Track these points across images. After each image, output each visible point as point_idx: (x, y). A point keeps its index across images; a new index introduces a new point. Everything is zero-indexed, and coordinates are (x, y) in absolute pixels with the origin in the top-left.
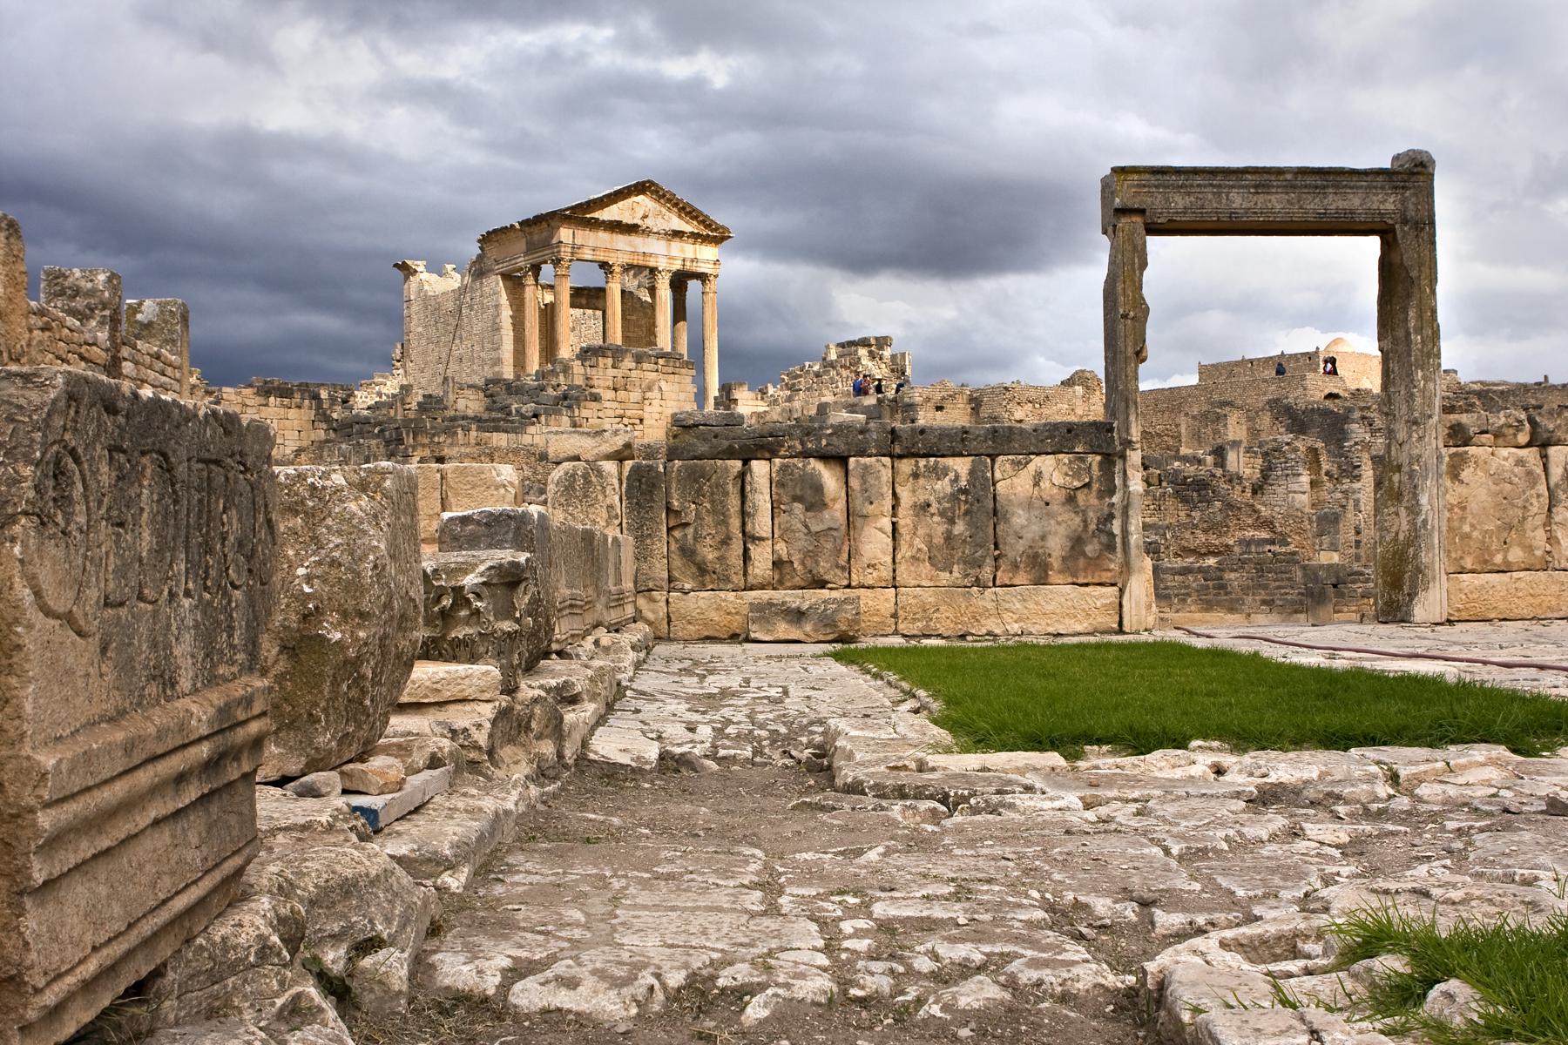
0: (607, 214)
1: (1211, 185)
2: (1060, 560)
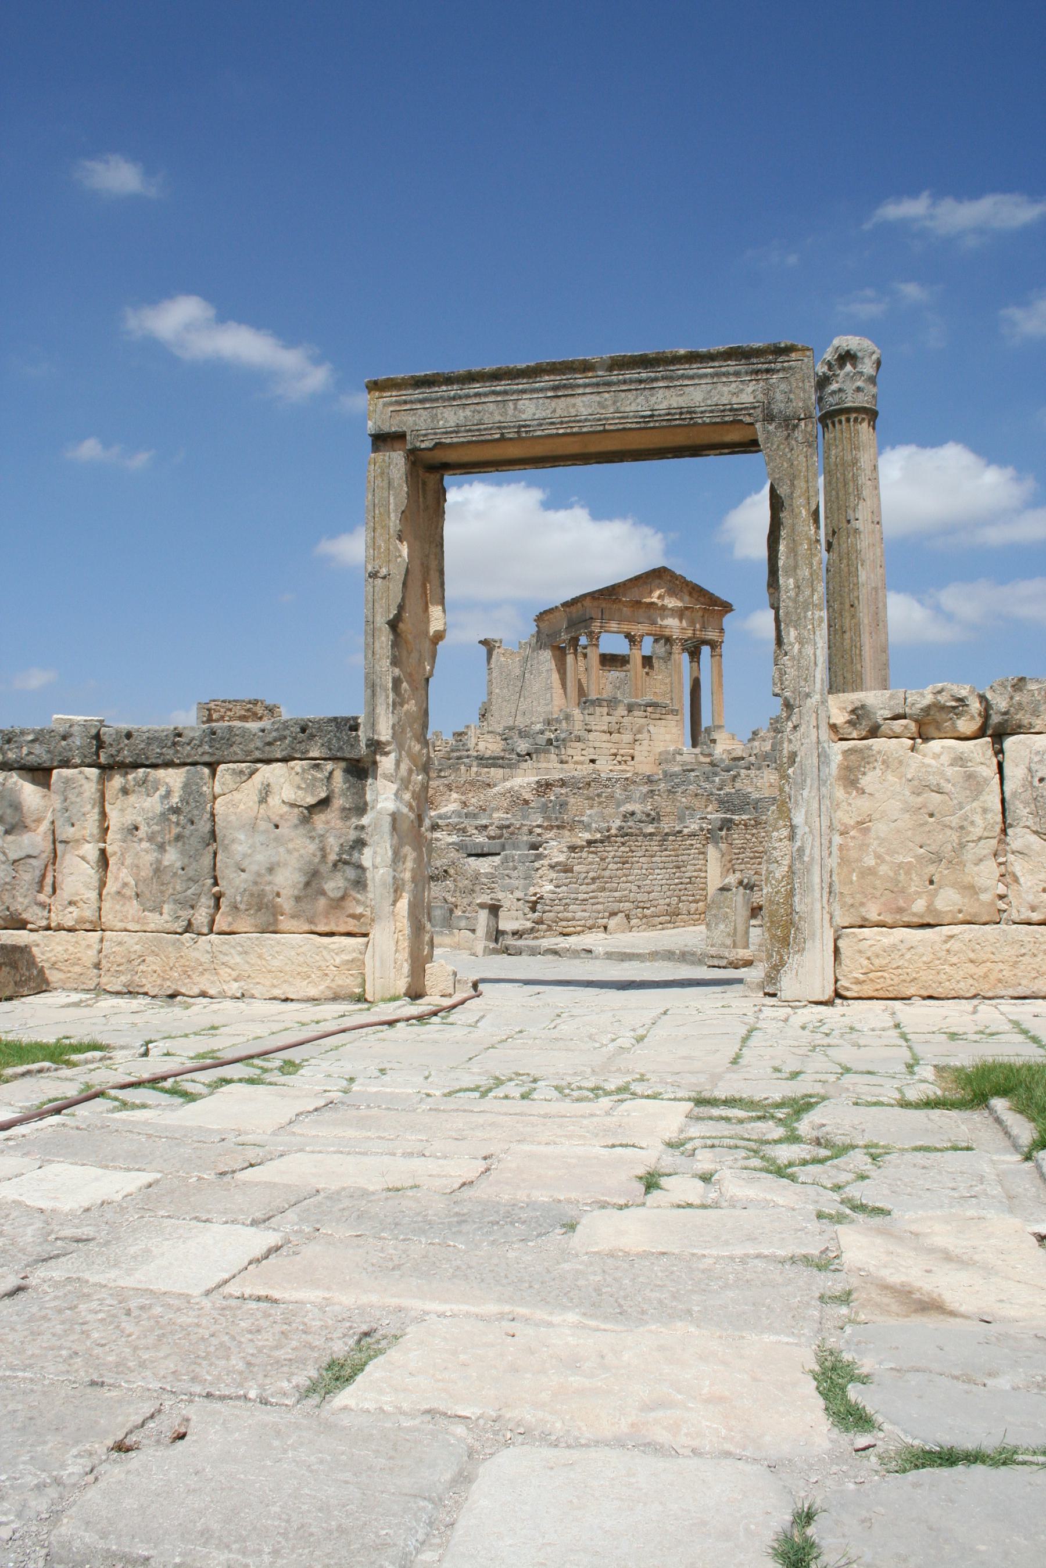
1: (494, 393)
2: (292, 902)
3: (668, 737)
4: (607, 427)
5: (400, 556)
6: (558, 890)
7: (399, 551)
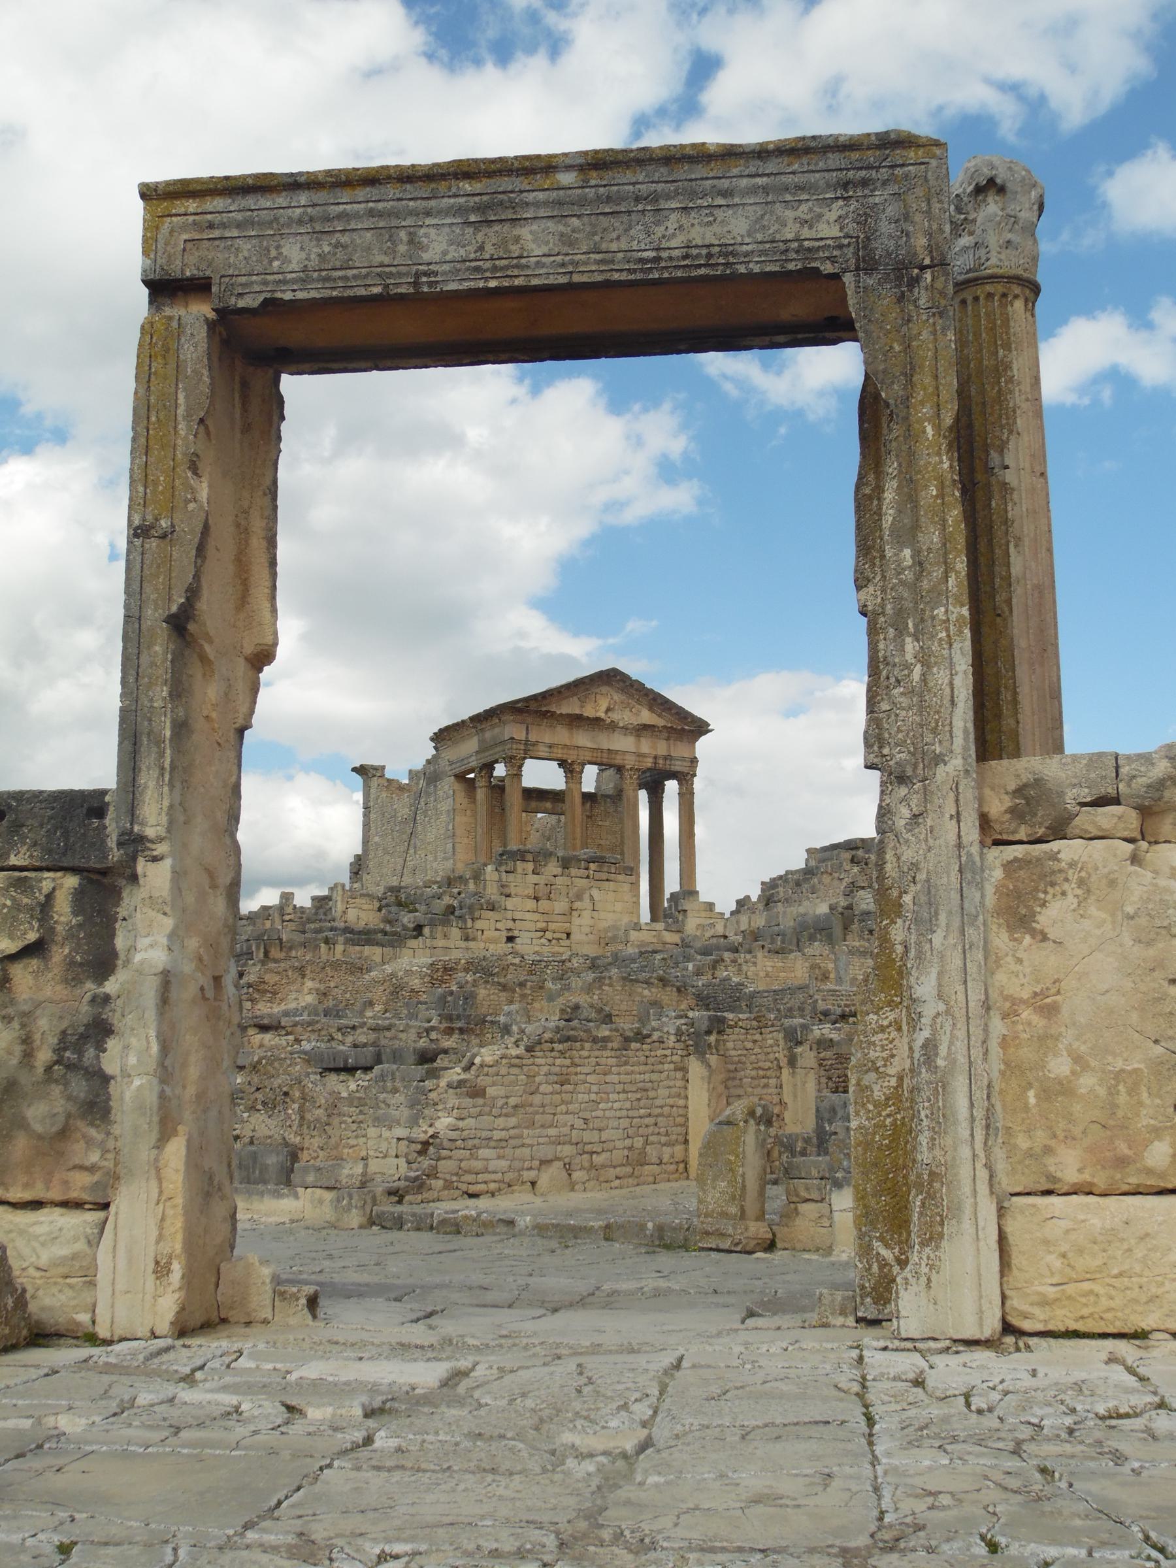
0: (569, 707)
1: (371, 213)
3: (619, 907)
4: (577, 278)
5: (195, 500)
6: (461, 1124)
7: (193, 491)
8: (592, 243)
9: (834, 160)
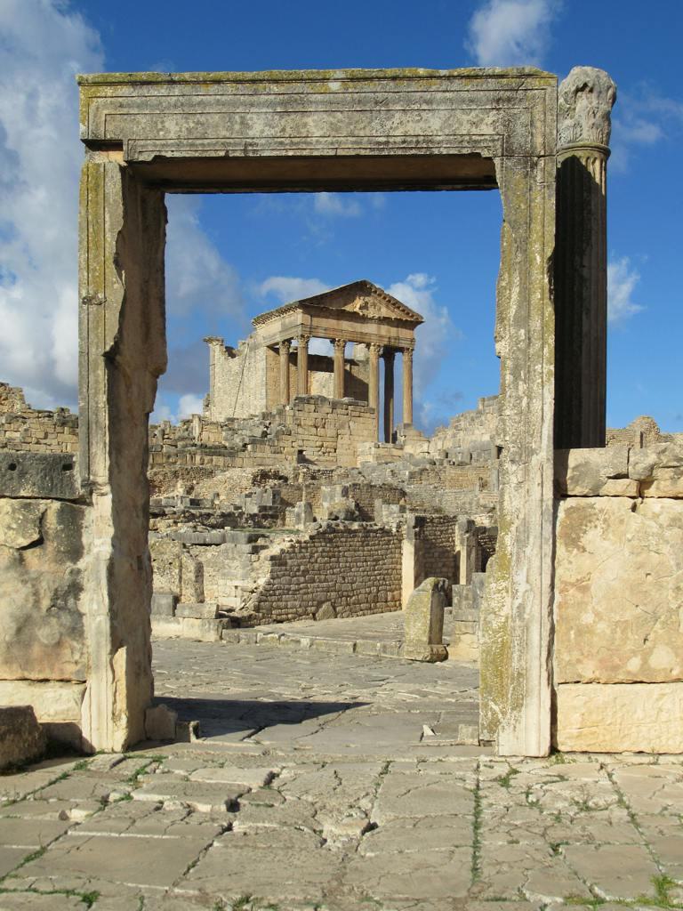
4: (340, 153)
8: (349, 130)
9: (492, 83)
